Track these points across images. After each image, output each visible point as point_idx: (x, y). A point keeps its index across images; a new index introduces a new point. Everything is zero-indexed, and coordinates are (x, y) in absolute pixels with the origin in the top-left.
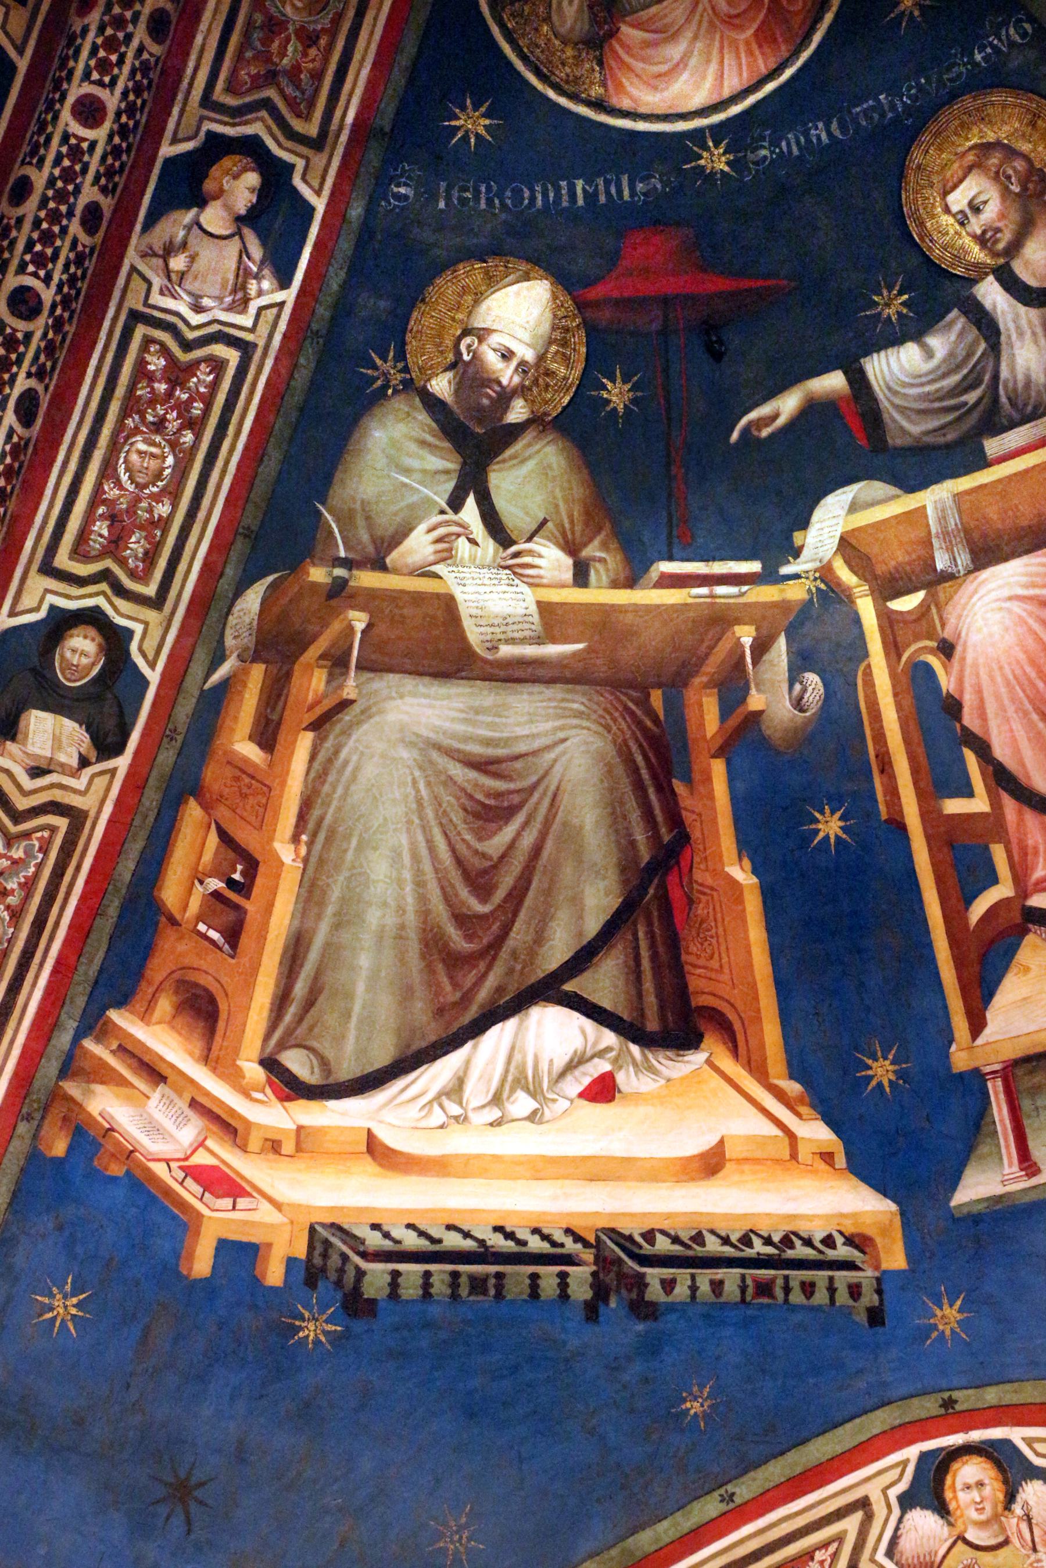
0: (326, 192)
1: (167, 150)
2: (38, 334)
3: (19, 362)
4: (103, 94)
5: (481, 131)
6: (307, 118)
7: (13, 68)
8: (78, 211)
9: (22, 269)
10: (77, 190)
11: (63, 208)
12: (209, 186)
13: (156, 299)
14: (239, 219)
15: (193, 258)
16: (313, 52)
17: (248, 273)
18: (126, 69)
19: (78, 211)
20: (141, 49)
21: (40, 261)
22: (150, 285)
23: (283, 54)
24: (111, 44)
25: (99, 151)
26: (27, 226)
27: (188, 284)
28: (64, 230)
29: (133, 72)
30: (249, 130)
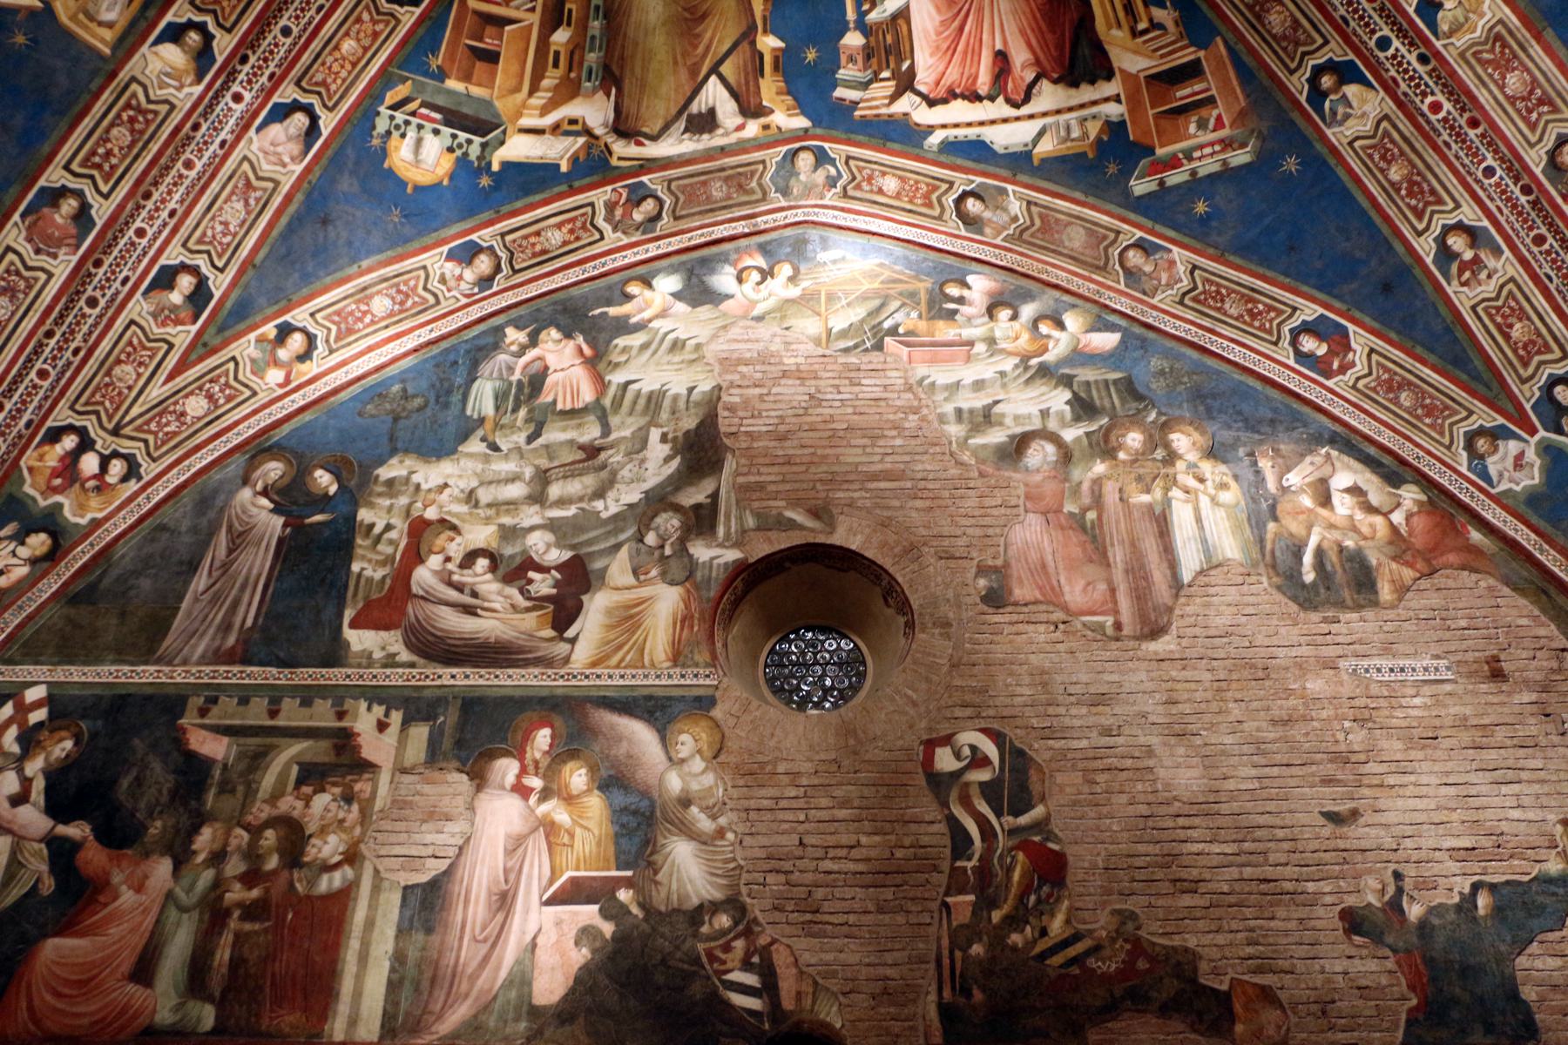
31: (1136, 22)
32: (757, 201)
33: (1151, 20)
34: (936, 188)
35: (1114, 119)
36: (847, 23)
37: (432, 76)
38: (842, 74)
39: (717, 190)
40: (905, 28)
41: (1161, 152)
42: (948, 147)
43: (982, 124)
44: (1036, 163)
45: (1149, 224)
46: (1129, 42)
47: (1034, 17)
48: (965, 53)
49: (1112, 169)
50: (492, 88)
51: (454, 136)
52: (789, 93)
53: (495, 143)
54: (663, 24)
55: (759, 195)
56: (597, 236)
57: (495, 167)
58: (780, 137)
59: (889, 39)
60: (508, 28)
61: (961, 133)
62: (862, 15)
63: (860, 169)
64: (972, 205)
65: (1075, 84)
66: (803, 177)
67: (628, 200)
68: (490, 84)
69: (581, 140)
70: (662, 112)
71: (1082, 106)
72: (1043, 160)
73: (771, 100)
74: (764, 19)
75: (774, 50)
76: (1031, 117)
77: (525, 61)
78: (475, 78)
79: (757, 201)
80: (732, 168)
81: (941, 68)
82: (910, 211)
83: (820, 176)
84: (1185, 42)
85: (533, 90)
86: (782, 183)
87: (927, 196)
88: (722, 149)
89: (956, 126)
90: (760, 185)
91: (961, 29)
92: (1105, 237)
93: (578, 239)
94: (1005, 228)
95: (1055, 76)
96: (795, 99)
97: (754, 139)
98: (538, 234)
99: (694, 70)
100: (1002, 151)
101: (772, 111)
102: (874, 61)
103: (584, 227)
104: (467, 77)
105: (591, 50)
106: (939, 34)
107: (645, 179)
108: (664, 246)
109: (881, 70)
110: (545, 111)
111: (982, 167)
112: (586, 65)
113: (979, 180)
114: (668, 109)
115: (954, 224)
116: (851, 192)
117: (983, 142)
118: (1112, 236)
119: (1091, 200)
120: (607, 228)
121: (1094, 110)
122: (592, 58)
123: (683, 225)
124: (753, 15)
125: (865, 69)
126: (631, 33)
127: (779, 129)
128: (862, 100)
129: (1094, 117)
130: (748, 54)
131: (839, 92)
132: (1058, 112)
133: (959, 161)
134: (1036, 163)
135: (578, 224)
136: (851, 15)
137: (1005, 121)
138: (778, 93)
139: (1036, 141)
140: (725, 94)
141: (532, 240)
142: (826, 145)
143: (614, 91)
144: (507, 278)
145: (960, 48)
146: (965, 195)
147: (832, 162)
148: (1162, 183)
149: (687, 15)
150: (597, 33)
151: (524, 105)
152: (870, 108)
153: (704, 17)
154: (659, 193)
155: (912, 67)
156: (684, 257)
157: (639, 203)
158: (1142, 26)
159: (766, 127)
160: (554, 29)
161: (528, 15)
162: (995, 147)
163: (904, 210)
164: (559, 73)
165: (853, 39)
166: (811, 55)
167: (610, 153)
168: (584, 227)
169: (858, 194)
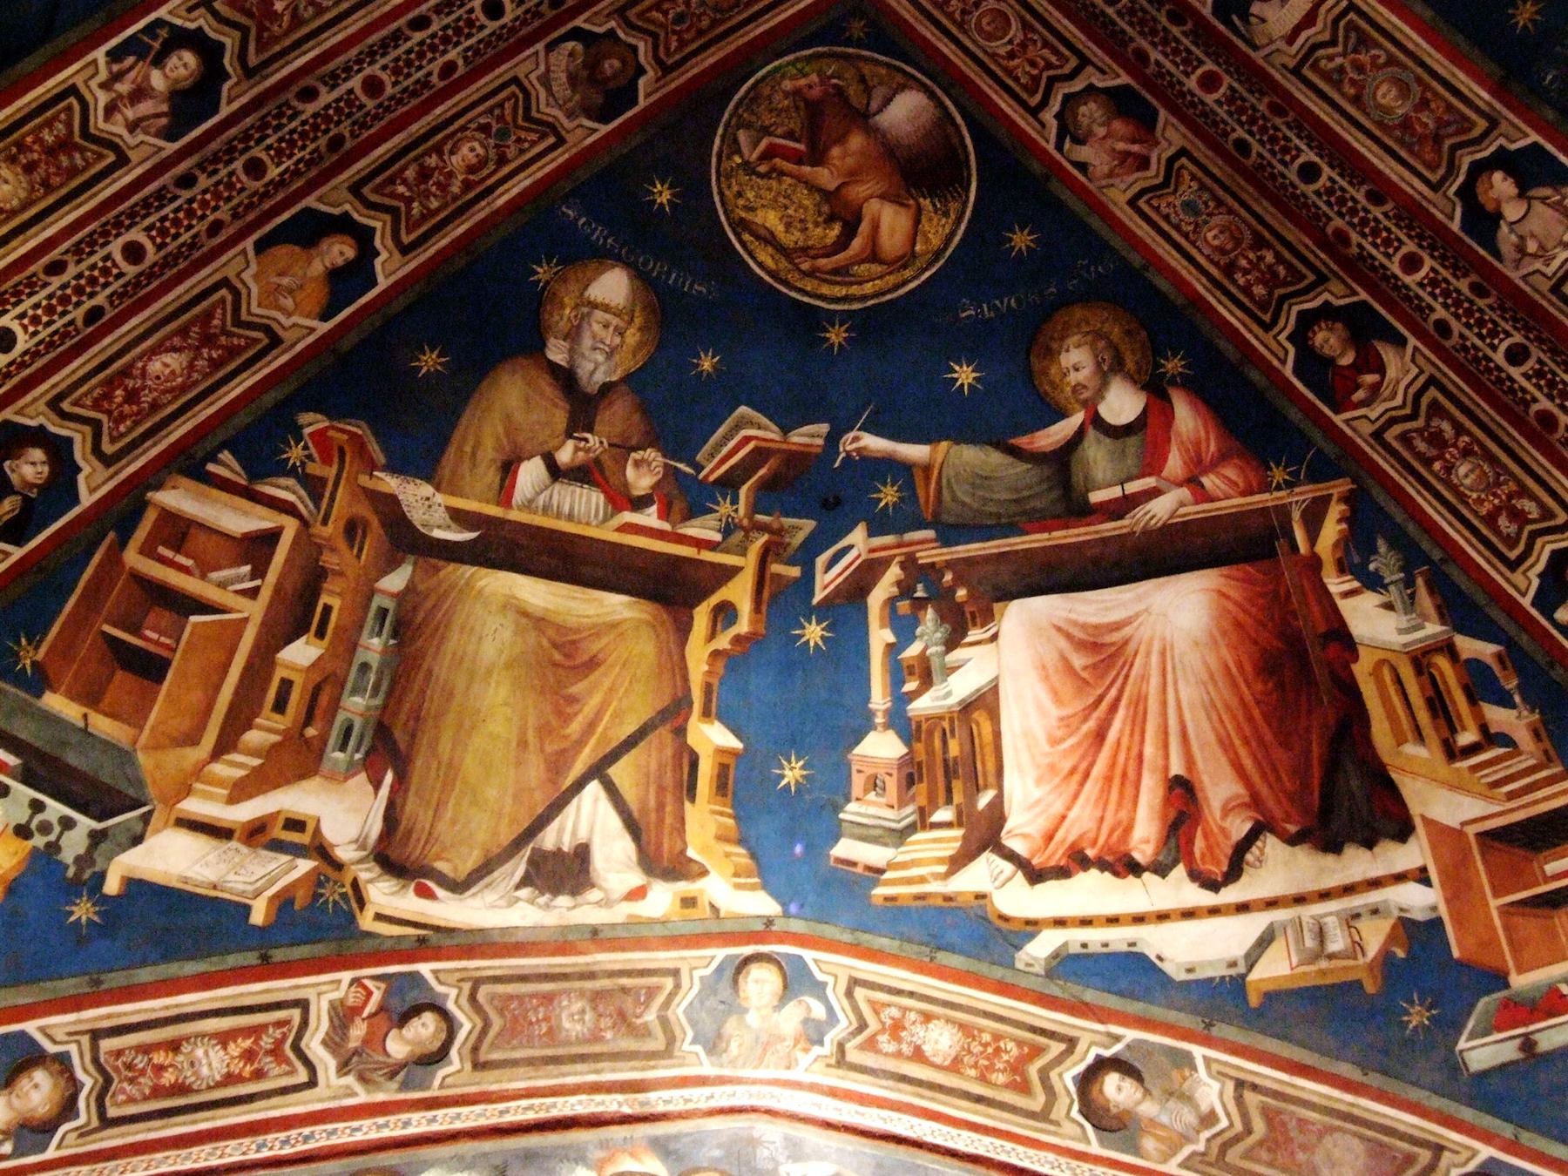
0: (1528, 130)
1: (1455, 226)
2: (1542, 356)
3: (1554, 374)
4: (1404, 250)
5: (1534, 9)
6: (1473, 124)
7: (1364, 302)
8: (1472, 297)
9: (1494, 348)
10: (1458, 291)
11: (1466, 305)
12: (1490, 207)
13: (1549, 271)
14: (1521, 195)
15: (1533, 236)
16: (1433, 105)
17: (1560, 203)
18: (1394, 229)
19: (1472, 297)
20: (1386, 214)
21: (1493, 333)
22: (1538, 271)
23: (1426, 125)
24: (1375, 233)
25: (1438, 267)
26: (1467, 332)
27: (1549, 245)
28: (1480, 310)
29: (1397, 225)
30: (1464, 168)
31: (1453, 731)
32: (653, 1055)
33: (1484, 728)
34: (1038, 1051)
35: (1419, 916)
36: (871, 714)
37: (19, 680)
38: (852, 812)
39: (573, 1019)
40: (986, 728)
41: (1520, 981)
42: (1065, 964)
43: (1139, 919)
44: (1254, 1000)
45: (1507, 1130)
46: (1442, 769)
47: (1250, 719)
48: (1108, 779)
49: (1417, 1017)
50: (141, 728)
51: (37, 806)
52: (741, 842)
53: (123, 839)
54: (509, 666)
55: (658, 1044)
56: (302, 1076)
57: (112, 886)
58: (714, 927)
59: (954, 748)
60: (194, 619)
61: (1095, 937)
62: (901, 700)
63: (877, 1008)
64: (1115, 1089)
65: (1332, 846)
66: (752, 1018)
67: (382, 1008)
68: (136, 717)
69: (305, 866)
70: (482, 836)
71: (1349, 890)
72: (1271, 997)
73: (704, 850)
74: (708, 690)
75: (721, 751)
76: (1243, 908)
77: (218, 688)
78: (104, 705)
79: (653, 1055)
80: (612, 974)
81: (1058, 807)
82: (979, 1099)
83: (790, 1018)
84: (1557, 769)
85: (225, 745)
86: (708, 1026)
87: (1017, 1068)
88: (595, 931)
89: (1086, 922)
90: (664, 1021)
91: (1100, 736)
92: (1410, 1160)
93: (259, 1075)
94: (1186, 1139)
95: (1292, 828)
96: (753, 856)
97: (663, 922)
98: (174, 1046)
99: (556, 765)
100: (1181, 976)
101: (704, 873)
102: (921, 789)
103: (276, 1052)
104: (91, 697)
105: (354, 692)
106: (1054, 742)
107: (425, 968)
108: (444, 1121)
109: (934, 806)
110: (240, 792)
111: (1135, 1007)
112: (341, 717)
113: (1131, 1034)
114: (495, 834)
115: (1074, 1130)
116: (853, 1056)
117: (1142, 957)
118: (1425, 1156)
119: (1375, 1080)
120: (326, 1063)
121: (1374, 897)
122: (356, 705)
123: (491, 1082)
124: (685, 679)
125: (902, 803)
126: (442, 669)
127: (714, 909)
128: (892, 866)
129: (1375, 912)
130: (669, 752)
131: (845, 848)
132: (1300, 900)
133: (1090, 996)
134: (1254, 1000)
135: (267, 1042)
136: (879, 700)
137: (1189, 914)
138: (721, 838)
139: (1252, 958)
140: (614, 821)
141: (159, 1058)
142: (809, 955)
143: (389, 777)
144: (84, 1133)
145: (1099, 769)
146: (1101, 1066)
147: (818, 989)
148: (1528, 1044)
149: (557, 657)
150: (374, 659)
151: (198, 772)
152: (909, 881)
153: (592, 664)
154: (451, 1006)
155: (998, 804)
156: (488, 1145)
157: (404, 1019)
158: (1467, 738)
159: (689, 902)
160: (289, 640)
161: (242, 602)
162: (1167, 967)
163: (967, 1096)
164: (282, 722)
165: (882, 747)
166: (792, 773)
167: (361, 903)
168: (276, 1052)
169: (869, 1060)
